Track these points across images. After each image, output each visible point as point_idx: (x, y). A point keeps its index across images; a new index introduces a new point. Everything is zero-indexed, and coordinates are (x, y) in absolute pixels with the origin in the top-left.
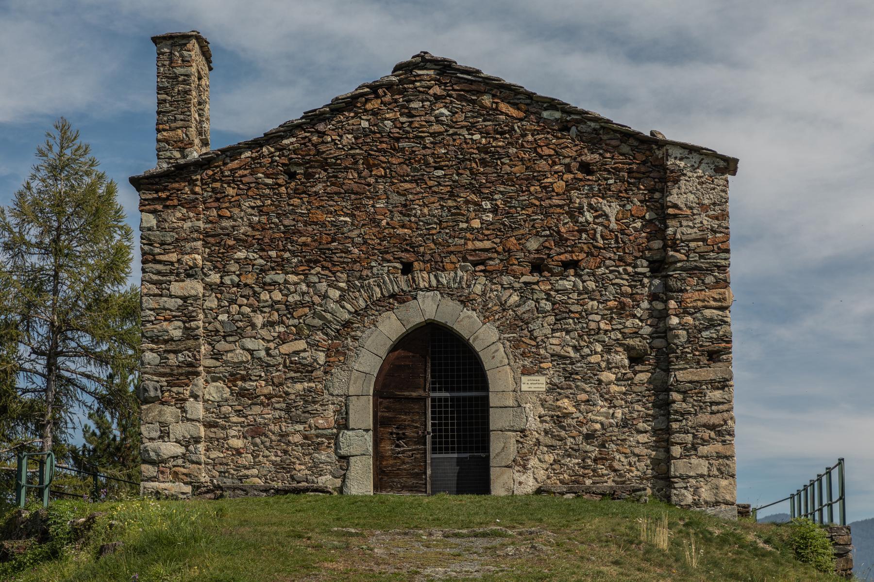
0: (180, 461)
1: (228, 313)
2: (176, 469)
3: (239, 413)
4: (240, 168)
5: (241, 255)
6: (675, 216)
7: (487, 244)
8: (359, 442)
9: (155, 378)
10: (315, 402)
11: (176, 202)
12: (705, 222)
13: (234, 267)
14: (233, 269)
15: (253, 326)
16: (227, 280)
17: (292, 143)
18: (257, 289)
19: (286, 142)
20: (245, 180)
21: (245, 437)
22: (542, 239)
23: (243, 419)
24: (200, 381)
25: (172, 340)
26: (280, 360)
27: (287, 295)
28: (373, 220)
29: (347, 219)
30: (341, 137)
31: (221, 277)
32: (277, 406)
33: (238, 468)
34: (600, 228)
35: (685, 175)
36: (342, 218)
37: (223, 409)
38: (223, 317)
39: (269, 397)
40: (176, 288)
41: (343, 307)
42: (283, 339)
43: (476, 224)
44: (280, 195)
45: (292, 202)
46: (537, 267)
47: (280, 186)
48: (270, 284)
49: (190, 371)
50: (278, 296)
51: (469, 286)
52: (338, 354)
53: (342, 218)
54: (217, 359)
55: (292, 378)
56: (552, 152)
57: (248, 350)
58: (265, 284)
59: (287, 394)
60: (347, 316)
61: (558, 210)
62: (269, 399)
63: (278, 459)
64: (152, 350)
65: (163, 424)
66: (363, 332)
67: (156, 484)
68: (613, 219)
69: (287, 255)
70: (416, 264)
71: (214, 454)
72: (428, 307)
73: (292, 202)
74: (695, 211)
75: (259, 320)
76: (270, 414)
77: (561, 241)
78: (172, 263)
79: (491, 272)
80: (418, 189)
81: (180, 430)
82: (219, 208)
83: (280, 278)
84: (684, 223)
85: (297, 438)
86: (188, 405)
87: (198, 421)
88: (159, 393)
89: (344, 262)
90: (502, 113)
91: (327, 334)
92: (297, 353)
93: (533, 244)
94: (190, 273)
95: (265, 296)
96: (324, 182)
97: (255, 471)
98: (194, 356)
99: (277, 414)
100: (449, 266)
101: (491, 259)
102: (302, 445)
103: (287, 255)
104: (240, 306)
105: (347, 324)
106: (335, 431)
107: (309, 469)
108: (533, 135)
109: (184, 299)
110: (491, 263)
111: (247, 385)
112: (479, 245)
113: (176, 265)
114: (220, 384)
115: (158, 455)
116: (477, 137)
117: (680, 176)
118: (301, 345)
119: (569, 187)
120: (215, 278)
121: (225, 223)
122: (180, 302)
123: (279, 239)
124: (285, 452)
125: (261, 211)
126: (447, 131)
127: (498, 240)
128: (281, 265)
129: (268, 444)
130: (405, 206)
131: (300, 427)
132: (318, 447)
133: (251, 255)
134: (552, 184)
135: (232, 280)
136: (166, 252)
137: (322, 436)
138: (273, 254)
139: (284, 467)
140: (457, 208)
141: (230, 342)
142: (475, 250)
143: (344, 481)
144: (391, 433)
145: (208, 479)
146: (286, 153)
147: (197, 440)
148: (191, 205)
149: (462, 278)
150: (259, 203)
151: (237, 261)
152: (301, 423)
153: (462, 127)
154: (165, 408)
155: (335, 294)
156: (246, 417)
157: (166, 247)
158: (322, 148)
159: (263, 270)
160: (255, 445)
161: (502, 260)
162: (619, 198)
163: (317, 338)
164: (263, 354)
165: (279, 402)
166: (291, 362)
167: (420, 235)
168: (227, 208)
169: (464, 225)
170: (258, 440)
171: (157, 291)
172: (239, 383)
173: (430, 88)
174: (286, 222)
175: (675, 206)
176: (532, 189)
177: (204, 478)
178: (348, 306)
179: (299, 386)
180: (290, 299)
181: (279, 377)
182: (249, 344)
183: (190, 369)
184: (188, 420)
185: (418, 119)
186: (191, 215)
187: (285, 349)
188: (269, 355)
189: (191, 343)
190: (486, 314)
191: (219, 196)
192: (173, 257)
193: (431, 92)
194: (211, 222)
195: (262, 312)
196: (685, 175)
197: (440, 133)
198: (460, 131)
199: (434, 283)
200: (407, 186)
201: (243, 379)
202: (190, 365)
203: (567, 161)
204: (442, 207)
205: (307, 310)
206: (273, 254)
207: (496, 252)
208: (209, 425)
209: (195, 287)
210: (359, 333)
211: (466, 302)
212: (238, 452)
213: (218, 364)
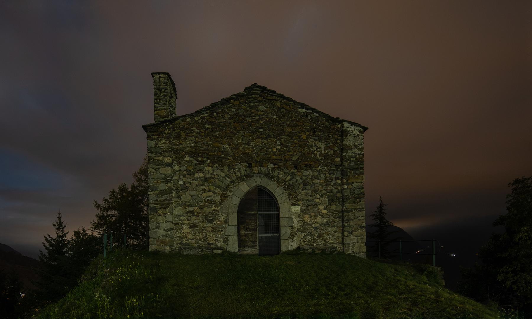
5: (187, 158)
7: (279, 157)
34: (318, 153)
42: (204, 191)
43: (275, 150)
50: (201, 175)
52: (224, 197)
69: (205, 159)
84: (349, 151)
93: (295, 158)
95: (196, 175)
118: (211, 193)
120: (176, 167)
133: (192, 159)
137: (219, 228)
138: (199, 159)
139: (205, 238)
155: (223, 174)
159: (196, 164)
169: (271, 150)
190: (279, 183)
209: (168, 170)
210: (232, 189)
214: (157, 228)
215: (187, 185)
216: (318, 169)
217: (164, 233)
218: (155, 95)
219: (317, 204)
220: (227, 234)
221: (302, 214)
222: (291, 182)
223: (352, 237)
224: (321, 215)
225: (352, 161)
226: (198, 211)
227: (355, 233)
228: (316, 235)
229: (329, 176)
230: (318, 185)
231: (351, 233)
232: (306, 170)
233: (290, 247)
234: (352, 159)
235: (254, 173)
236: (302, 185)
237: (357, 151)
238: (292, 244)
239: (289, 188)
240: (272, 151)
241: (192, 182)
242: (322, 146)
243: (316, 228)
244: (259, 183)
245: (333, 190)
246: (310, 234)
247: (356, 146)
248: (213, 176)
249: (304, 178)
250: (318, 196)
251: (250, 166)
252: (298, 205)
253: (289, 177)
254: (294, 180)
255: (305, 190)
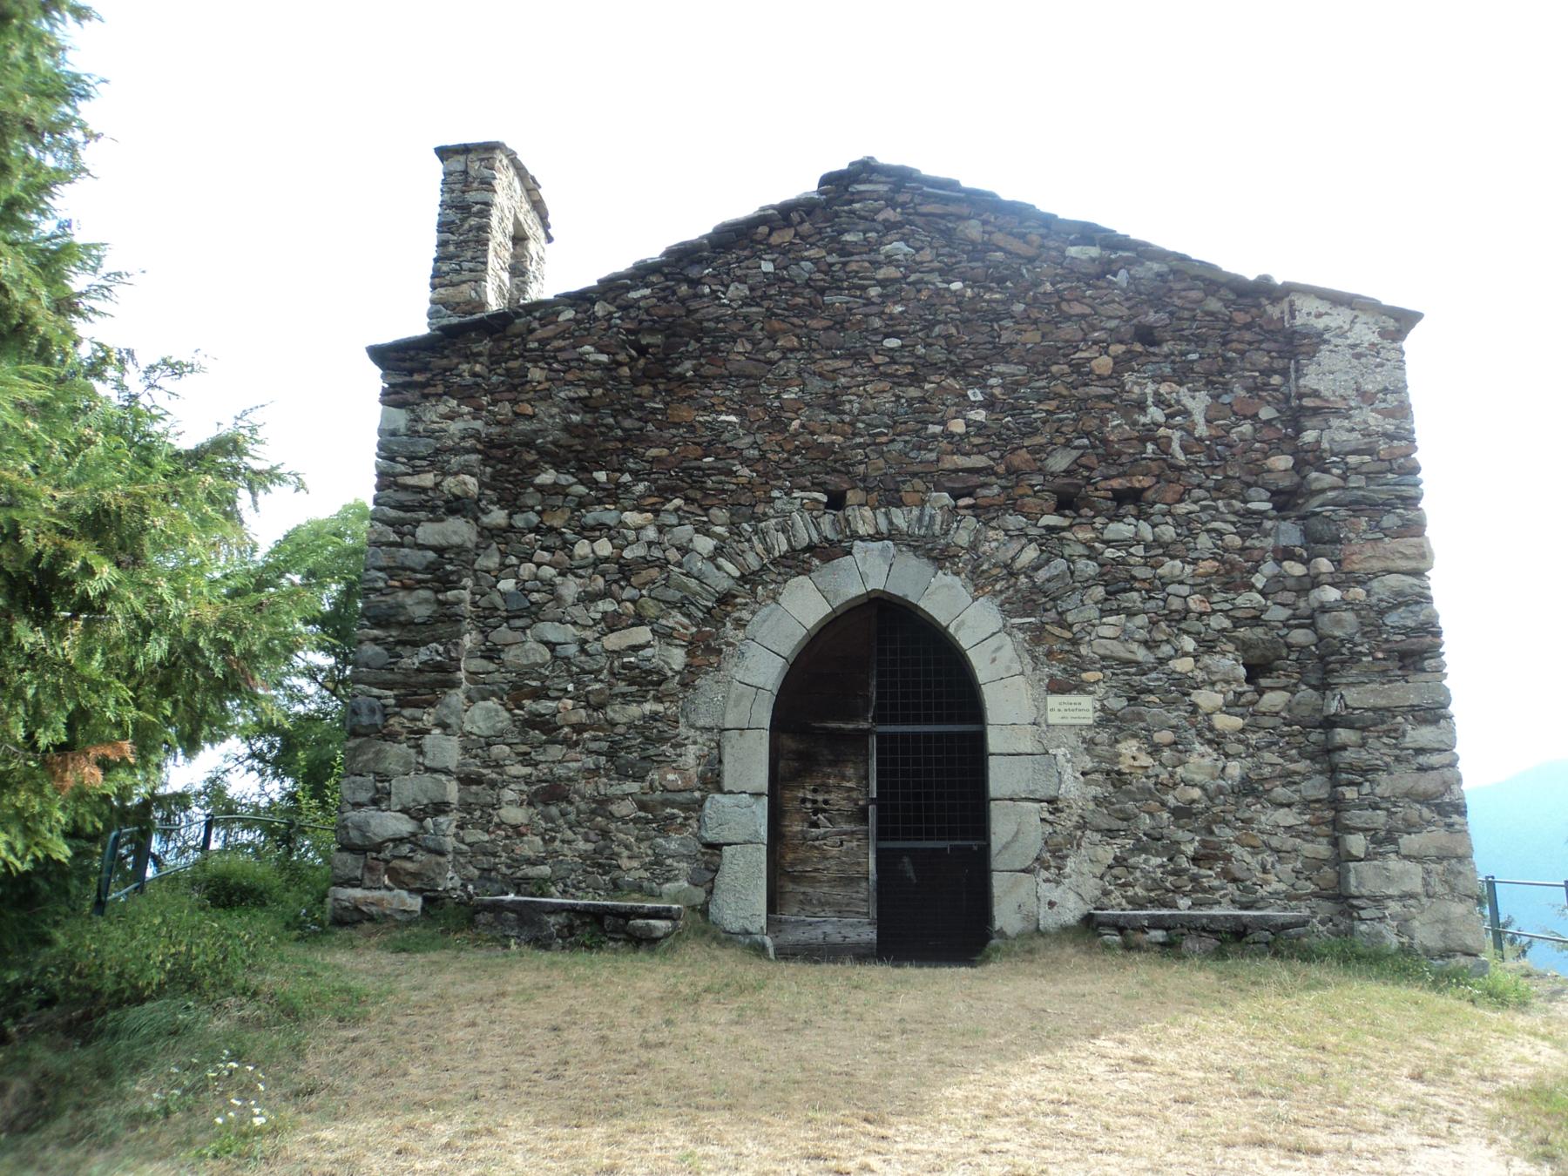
0: (405, 849)
1: (516, 576)
2: (396, 863)
3: (525, 759)
4: (555, 337)
5: (547, 477)
6: (1316, 411)
7: (979, 461)
8: (741, 816)
9: (375, 691)
10: (664, 740)
11: (440, 389)
12: (1371, 421)
13: (531, 498)
14: (530, 502)
15: (558, 599)
16: (519, 521)
17: (644, 297)
18: (569, 535)
19: (634, 295)
20: (561, 356)
21: (530, 804)
22: (1075, 453)
23: (528, 770)
24: (457, 697)
25: (411, 622)
26: (603, 661)
27: (622, 548)
28: (776, 420)
29: (733, 418)
30: (727, 287)
31: (510, 516)
32: (594, 746)
33: (516, 862)
34: (1176, 435)
35: (1327, 342)
36: (723, 418)
37: (495, 750)
38: (507, 585)
39: (579, 728)
40: (428, 532)
41: (719, 568)
42: (612, 623)
43: (958, 426)
44: (618, 379)
45: (638, 391)
46: (1066, 502)
47: (620, 364)
48: (593, 529)
49: (442, 676)
50: (604, 548)
51: (946, 533)
52: (706, 651)
53: (723, 418)
54: (491, 659)
55: (624, 695)
56: (1088, 310)
57: (547, 643)
58: (584, 528)
59: (613, 724)
60: (724, 584)
61: (1103, 404)
62: (579, 733)
63: (590, 846)
64: (375, 640)
65: (384, 777)
66: (754, 613)
67: (358, 893)
68: (1199, 418)
69: (626, 478)
70: (849, 494)
71: (476, 835)
72: (870, 570)
73: (638, 391)
74: (1353, 404)
75: (570, 588)
76: (578, 761)
77: (1109, 456)
78: (424, 490)
79: (987, 508)
80: (856, 370)
81: (409, 788)
82: (514, 402)
83: (608, 515)
84: (1335, 422)
85: (626, 808)
86: (427, 741)
87: (447, 772)
88: (378, 719)
89: (724, 491)
90: (1000, 249)
91: (688, 616)
92: (635, 648)
93: (1060, 462)
94: (457, 506)
95: (582, 548)
96: (697, 358)
97: (545, 870)
98: (447, 651)
99: (590, 762)
100: (907, 498)
101: (984, 485)
102: (636, 820)
103: (626, 478)
104: (539, 565)
105: (725, 599)
106: (697, 794)
107: (645, 867)
108: (1053, 284)
109: (440, 550)
110: (986, 492)
111: (545, 706)
112: (960, 461)
113: (431, 493)
114: (493, 703)
115: (364, 835)
116: (956, 286)
117: (1318, 344)
118: (642, 634)
119: (1121, 364)
120: (498, 516)
121: (523, 426)
122: (431, 555)
123: (615, 451)
124: (605, 834)
125: (586, 405)
126: (905, 277)
127: (996, 454)
128: (613, 494)
129: (572, 817)
130: (834, 396)
131: (632, 787)
132: (665, 826)
133: (566, 479)
134: (1089, 360)
135: (527, 521)
136: (417, 471)
137: (673, 804)
138: (601, 476)
139: (601, 862)
140: (923, 400)
141: (516, 629)
142: (956, 471)
143: (710, 892)
144: (804, 800)
145: (457, 882)
146: (633, 313)
147: (440, 808)
148: (466, 394)
149: (932, 517)
150: (583, 393)
151: (541, 489)
152: (636, 778)
153: (931, 271)
154: (387, 746)
155: (705, 544)
156: (536, 765)
157: (418, 463)
158: (694, 305)
159: (582, 503)
160: (548, 818)
161: (1004, 488)
162: (1209, 383)
163: (671, 623)
164: (572, 650)
165: (595, 739)
166: (624, 666)
167: (859, 446)
168: (528, 401)
169: (938, 429)
170: (554, 810)
171: (394, 537)
172: (526, 702)
173: (877, 211)
174: (628, 423)
175: (1315, 394)
176: (1054, 368)
177: (450, 881)
178: (729, 567)
179: (634, 710)
180: (628, 554)
181: (600, 691)
182: (551, 632)
183: (439, 676)
184: (428, 769)
185: (856, 258)
186: (465, 409)
187: (614, 641)
188: (583, 651)
189: (442, 629)
190: (979, 580)
191: (516, 381)
192: (428, 480)
193: (880, 217)
194: (499, 423)
195: (577, 576)
196: (1327, 342)
197: (894, 281)
198: (927, 277)
199: (883, 527)
200: (839, 364)
201: (539, 694)
202: (439, 667)
203: (1113, 324)
204: (898, 397)
205: (654, 572)
206: (601, 476)
207: (995, 474)
208: (466, 780)
210: (745, 615)
211: (941, 557)
212: (517, 831)
213: (492, 667)
214: (375, 802)
215: (535, 597)
216: (1182, 508)
217: (405, 826)
218: (444, 226)
219: (1184, 685)
220: (710, 836)
221: (1103, 736)
222: (1041, 576)
223: (1394, 864)
224: (1210, 742)
225: (1356, 470)
226: (574, 719)
227: (1409, 842)
228: (1190, 850)
229: (1238, 541)
230: (1184, 590)
231: (1384, 840)
232: (1118, 518)
233: (1044, 908)
234: (1353, 460)
235: (855, 536)
236: (1099, 592)
237: (1374, 420)
238: (1055, 894)
239: (1032, 606)
240: (950, 436)
241: (558, 580)
242: (1198, 403)
243: (1182, 813)
244: (877, 583)
245: (1264, 610)
246: (1155, 841)
247: (1366, 397)
248: (657, 553)
249: (1110, 553)
250: (1189, 644)
251: (836, 502)
252: (1080, 688)
253: (1031, 554)
254: (1059, 565)
255: (1117, 612)
